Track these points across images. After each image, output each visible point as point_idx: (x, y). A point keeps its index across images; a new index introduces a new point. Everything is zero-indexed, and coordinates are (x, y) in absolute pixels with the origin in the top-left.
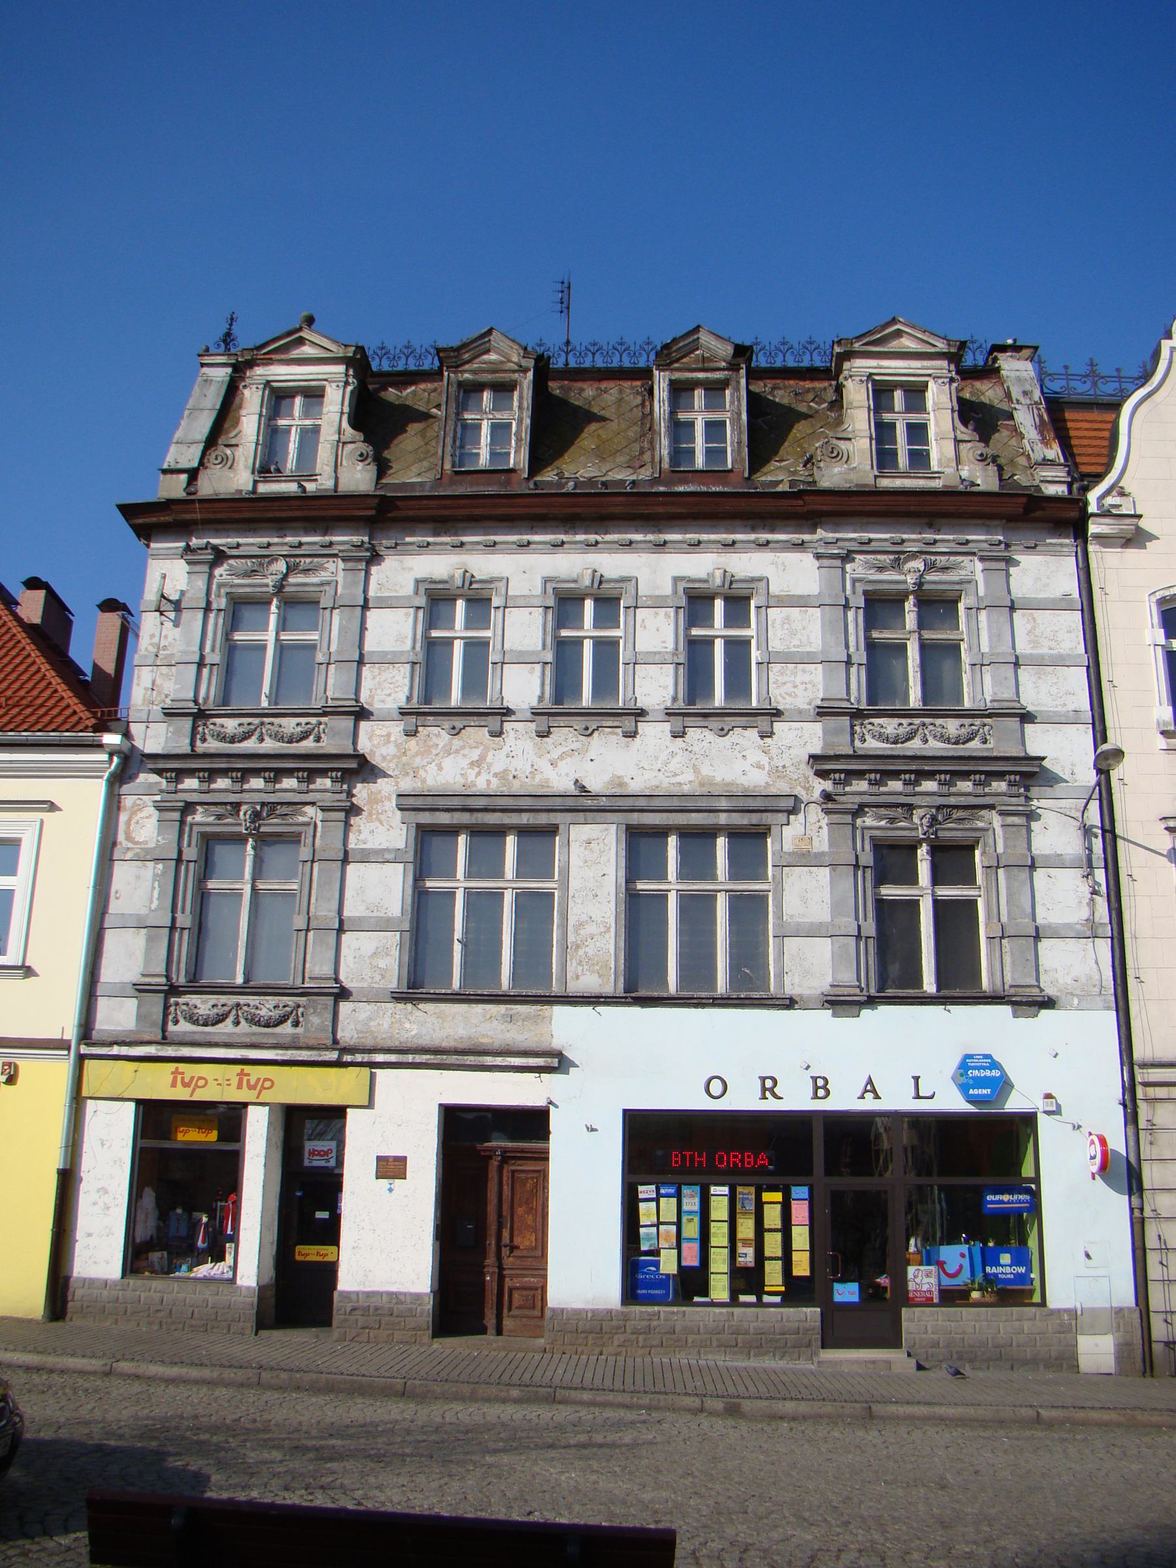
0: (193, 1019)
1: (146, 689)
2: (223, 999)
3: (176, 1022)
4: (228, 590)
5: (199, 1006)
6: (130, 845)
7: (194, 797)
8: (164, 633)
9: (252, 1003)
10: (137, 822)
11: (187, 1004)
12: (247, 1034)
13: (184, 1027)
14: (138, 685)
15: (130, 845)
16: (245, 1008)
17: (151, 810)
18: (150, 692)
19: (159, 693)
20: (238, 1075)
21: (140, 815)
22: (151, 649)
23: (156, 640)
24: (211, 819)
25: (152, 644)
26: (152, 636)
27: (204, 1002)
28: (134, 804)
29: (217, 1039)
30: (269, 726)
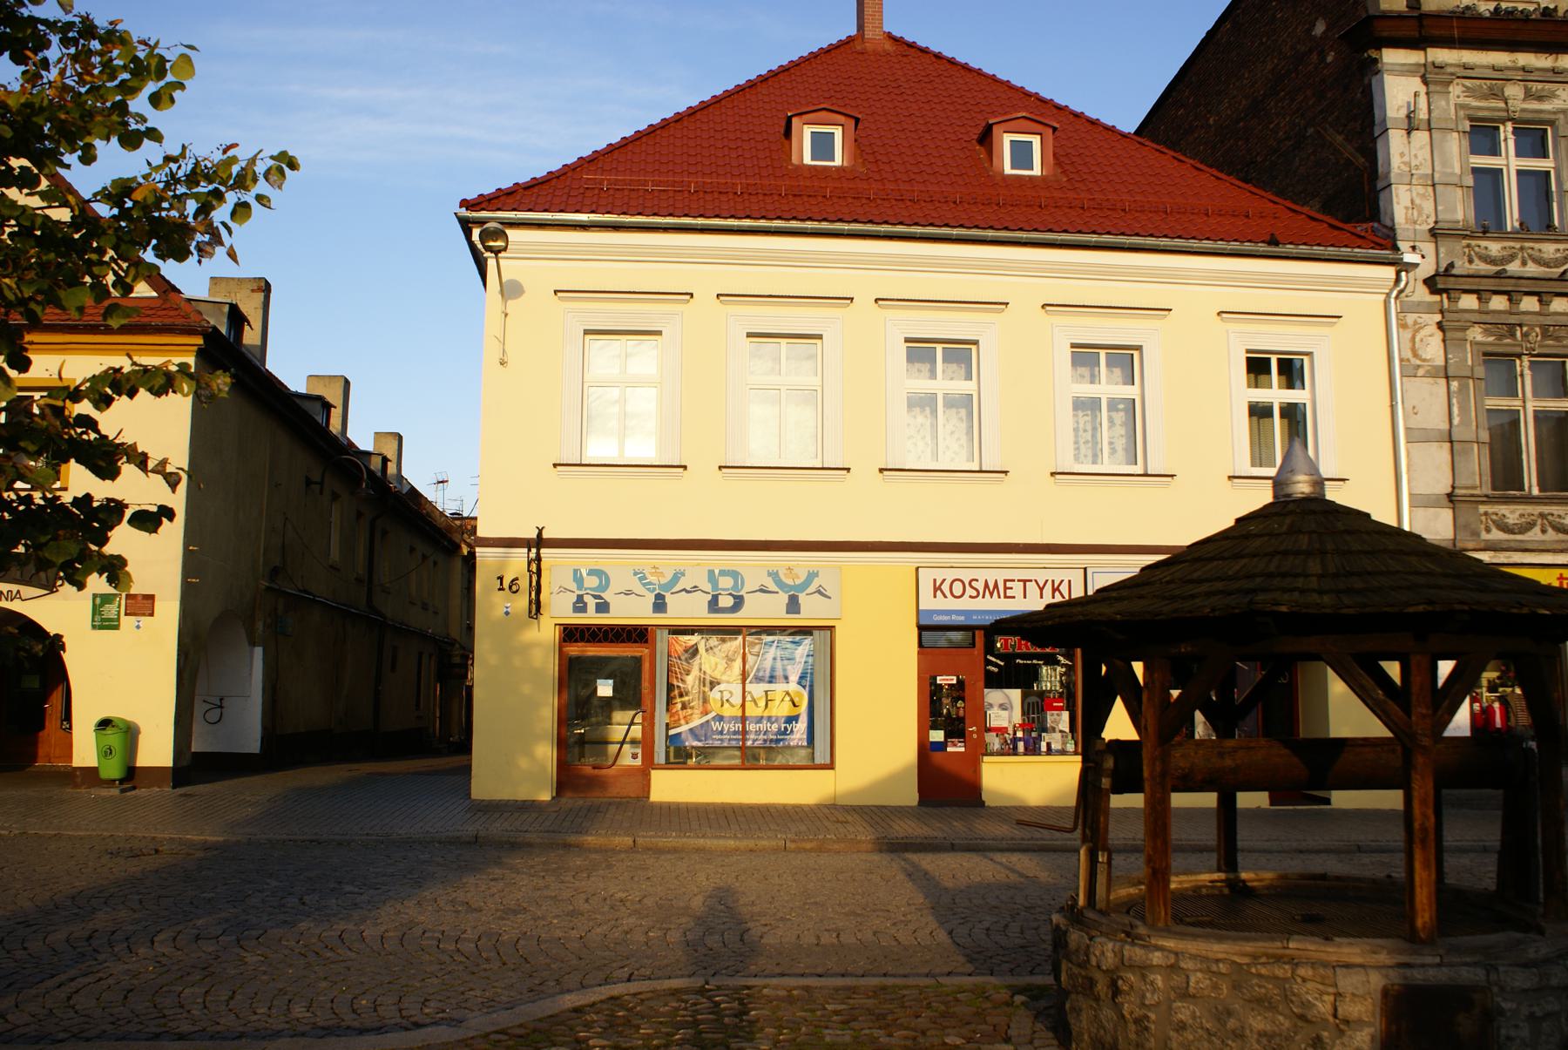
0: (1505, 528)
1: (1407, 208)
2: (1529, 509)
3: (1488, 530)
4: (1467, 112)
5: (1508, 515)
6: (1418, 362)
7: (1477, 317)
8: (1413, 153)
9: (1556, 513)
10: (1422, 340)
11: (1497, 514)
12: (1557, 541)
13: (1496, 535)
14: (1398, 203)
15: (1418, 362)
16: (1550, 518)
17: (1433, 329)
18: (1410, 211)
19: (1420, 214)
20: (1558, 579)
21: (1423, 333)
22: (1403, 167)
23: (1406, 159)
24: (1491, 339)
25: (1403, 163)
26: (1402, 155)
27: (1512, 512)
28: (1415, 323)
29: (1529, 546)
30: (1530, 251)
